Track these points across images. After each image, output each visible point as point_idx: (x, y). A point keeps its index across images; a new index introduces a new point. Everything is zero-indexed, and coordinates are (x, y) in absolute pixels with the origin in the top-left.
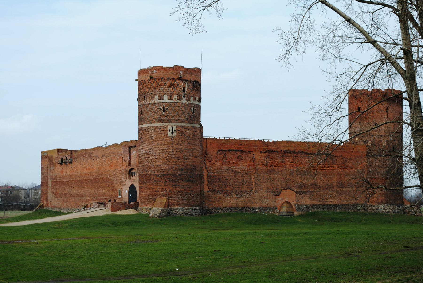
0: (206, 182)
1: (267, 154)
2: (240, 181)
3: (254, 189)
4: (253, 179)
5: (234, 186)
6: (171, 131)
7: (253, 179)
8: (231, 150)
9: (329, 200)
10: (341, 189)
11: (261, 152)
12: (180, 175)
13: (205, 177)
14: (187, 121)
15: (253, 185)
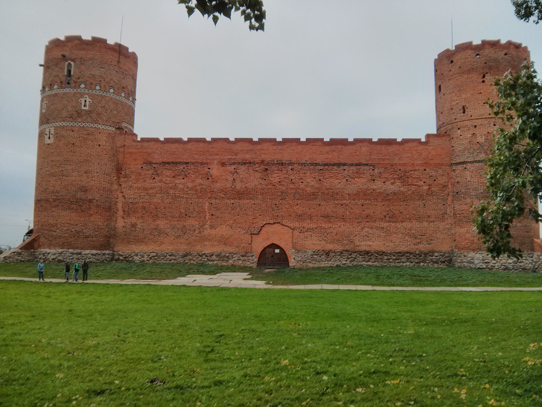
0: (120, 213)
1: (233, 167)
2: (183, 211)
3: (208, 223)
4: (206, 208)
5: (170, 218)
6: (48, 135)
7: (206, 208)
8: (168, 163)
9: (363, 243)
10: (393, 224)
11: (223, 164)
12: (55, 200)
13: (120, 205)
14: (71, 119)
15: (207, 217)
